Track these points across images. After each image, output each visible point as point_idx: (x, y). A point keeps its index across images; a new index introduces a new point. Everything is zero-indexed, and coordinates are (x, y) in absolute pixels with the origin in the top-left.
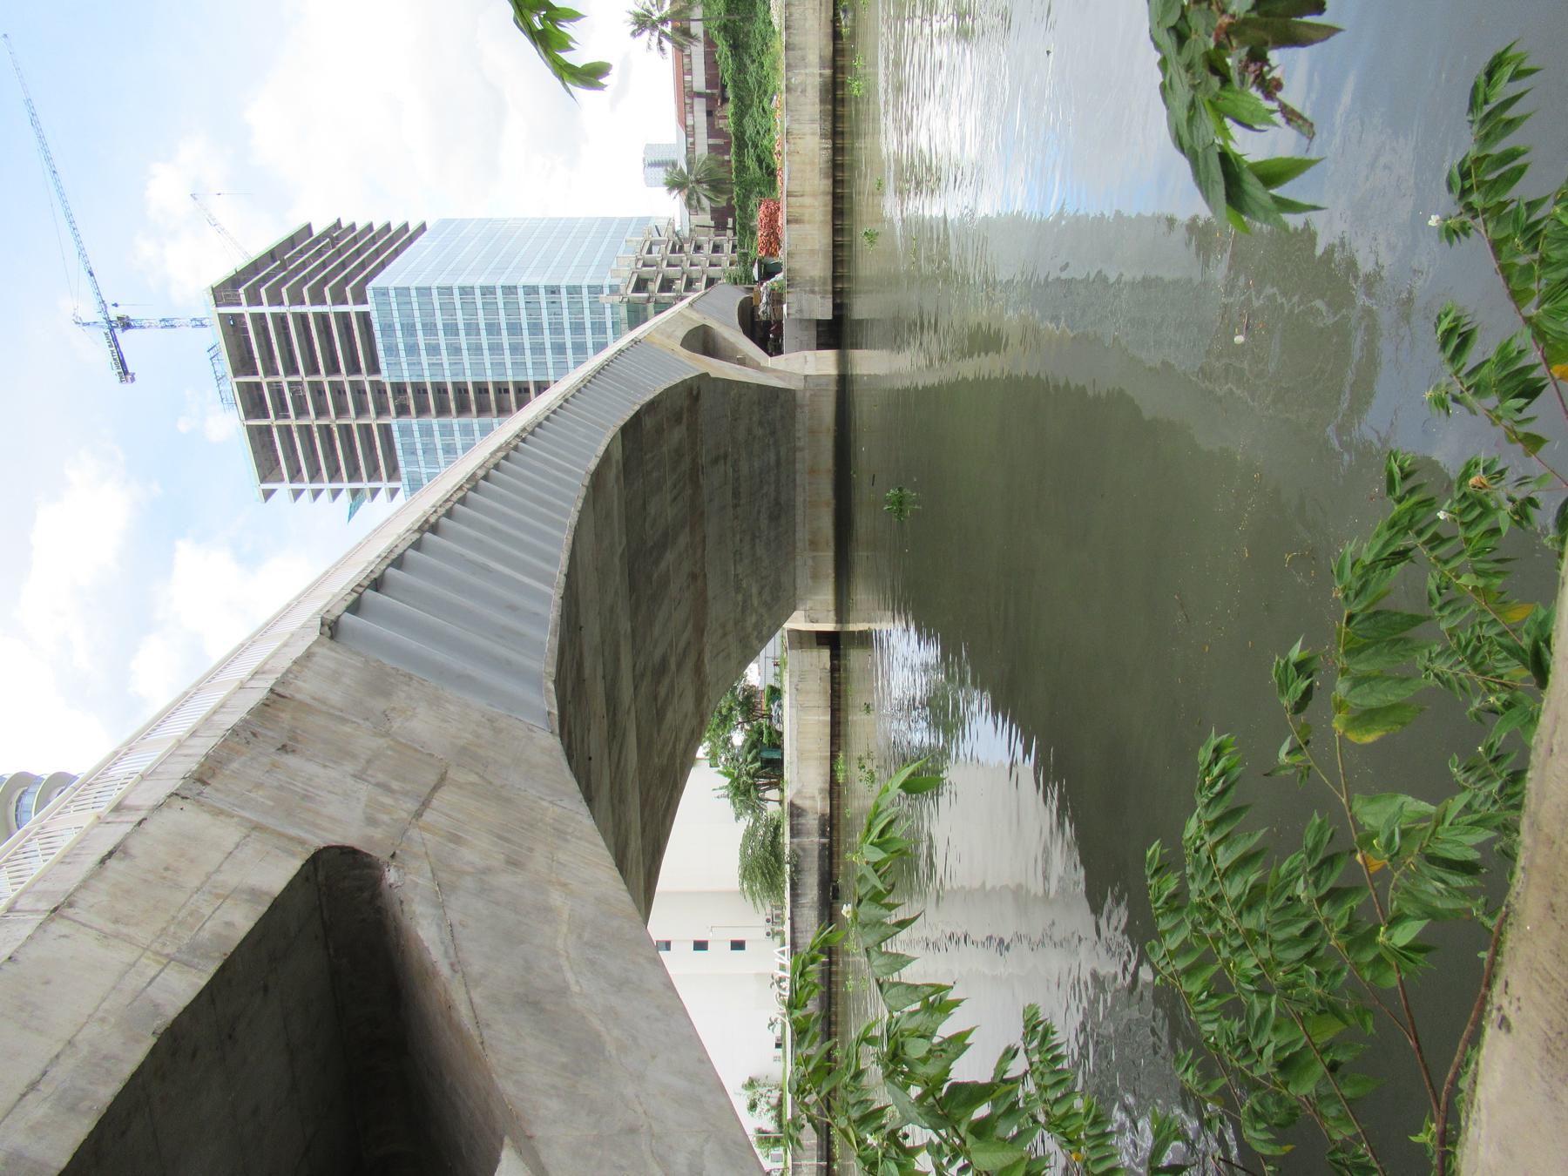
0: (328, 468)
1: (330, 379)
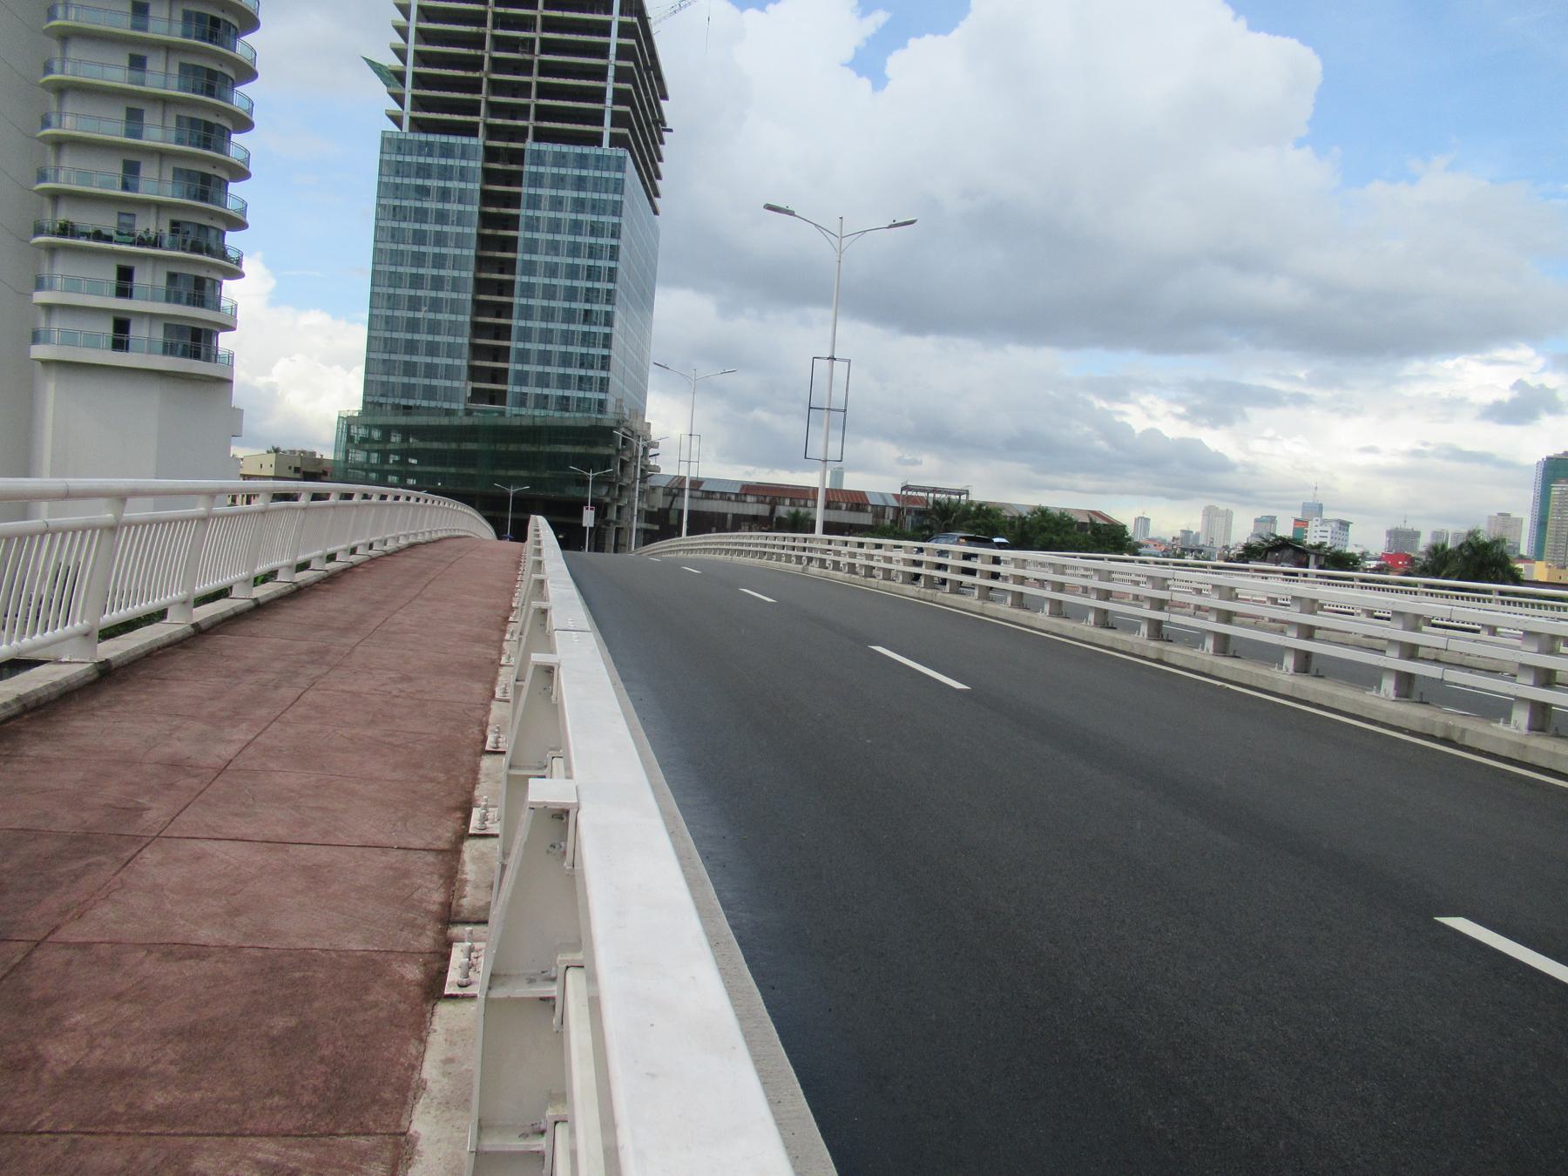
0: (431, 53)
1: (534, 84)
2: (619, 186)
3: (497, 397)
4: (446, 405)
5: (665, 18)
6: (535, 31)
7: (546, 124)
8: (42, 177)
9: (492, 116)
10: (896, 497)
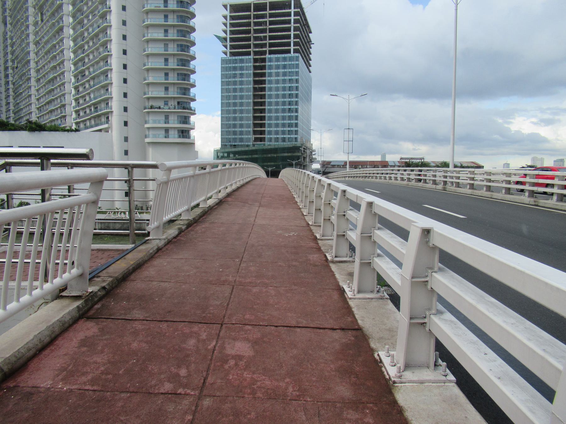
0: (234, 30)
1: (268, 36)
2: (297, 66)
3: (262, 140)
4: (247, 144)
5: (308, 7)
6: (267, 18)
7: (272, 49)
8: (145, 94)
9: (255, 48)
10: (399, 162)
